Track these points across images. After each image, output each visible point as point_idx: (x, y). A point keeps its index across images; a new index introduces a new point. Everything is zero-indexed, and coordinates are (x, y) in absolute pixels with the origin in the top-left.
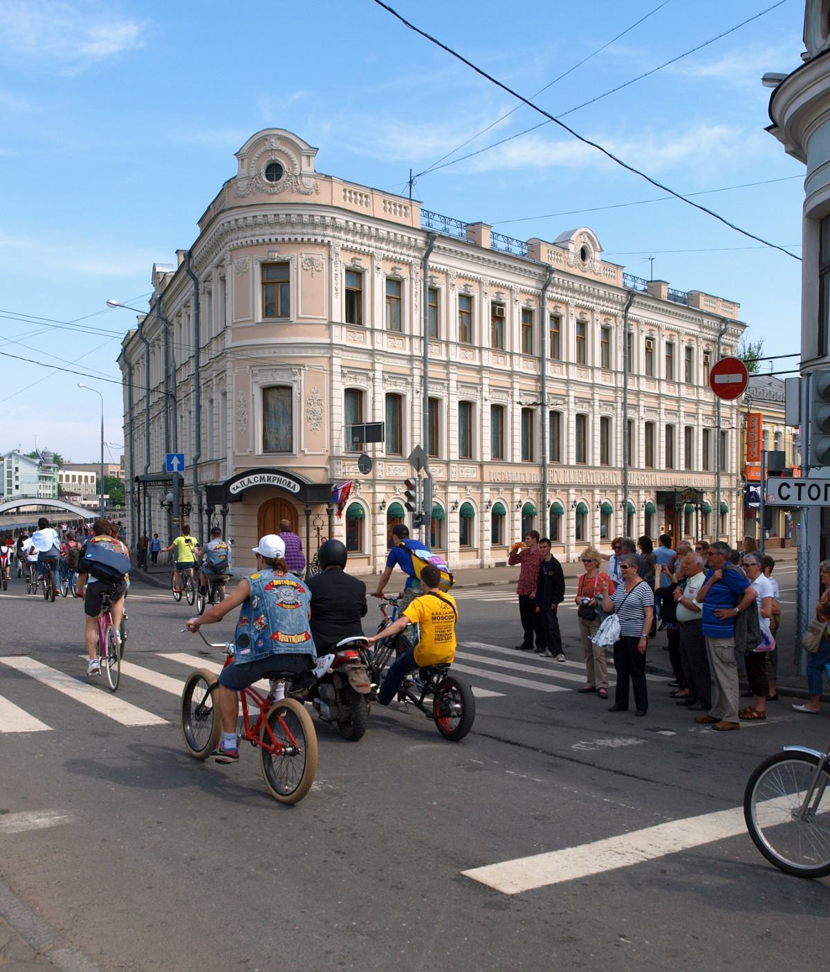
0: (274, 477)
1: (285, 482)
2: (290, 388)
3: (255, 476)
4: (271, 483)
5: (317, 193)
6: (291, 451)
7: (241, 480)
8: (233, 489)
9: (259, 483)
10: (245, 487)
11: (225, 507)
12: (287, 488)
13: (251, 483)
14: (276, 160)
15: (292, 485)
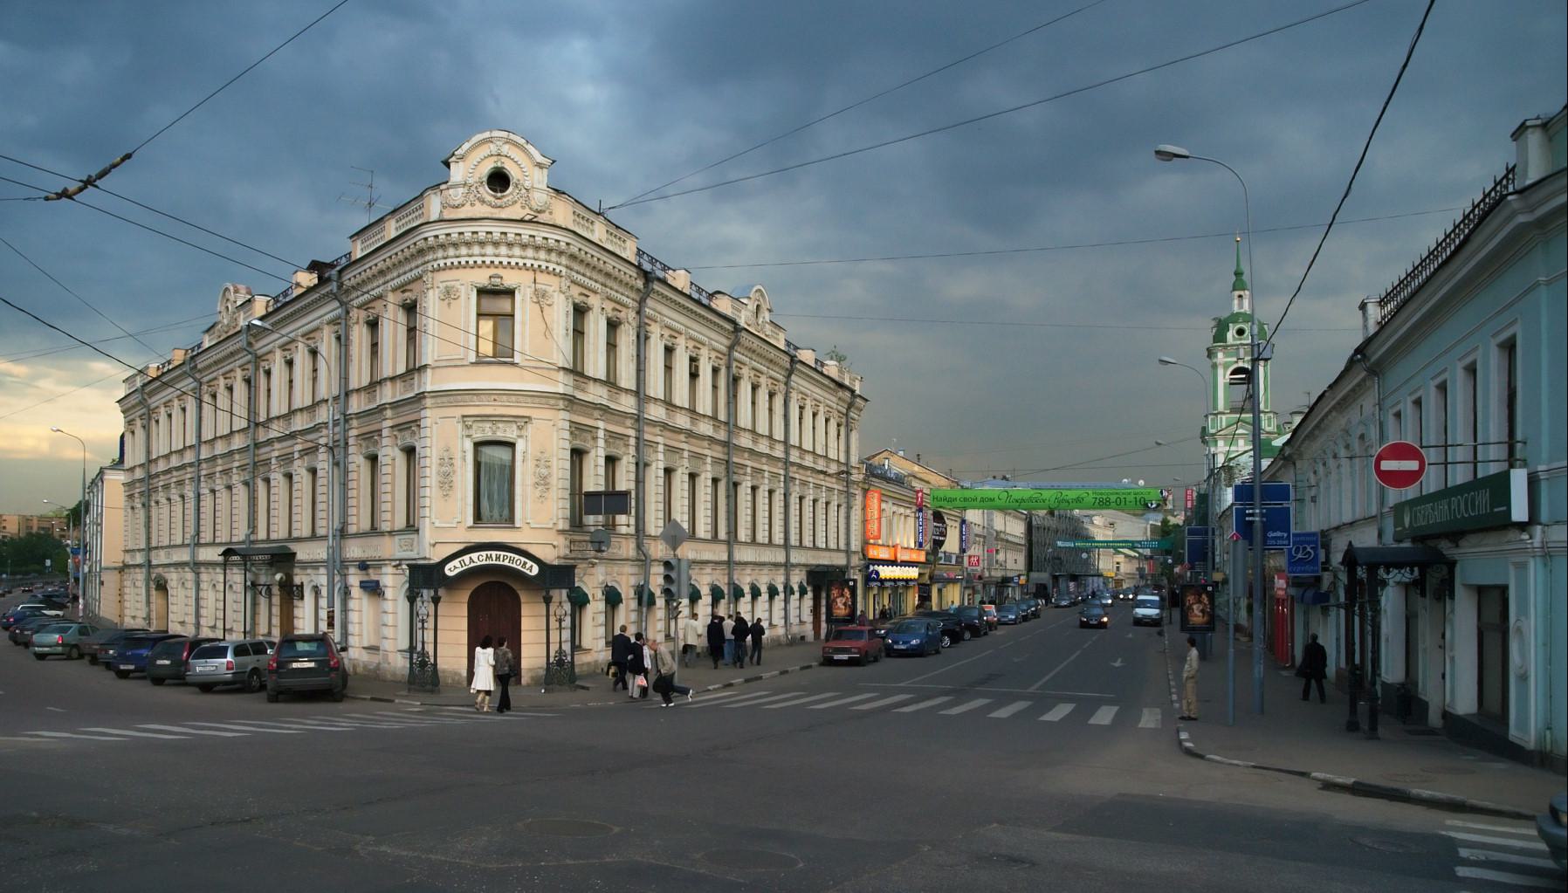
0: (504, 556)
1: (519, 562)
2: (512, 445)
3: (479, 553)
4: (501, 563)
5: (551, 213)
7: (460, 559)
8: (450, 569)
9: (484, 563)
10: (465, 568)
11: (436, 592)
12: (522, 569)
15: (527, 566)
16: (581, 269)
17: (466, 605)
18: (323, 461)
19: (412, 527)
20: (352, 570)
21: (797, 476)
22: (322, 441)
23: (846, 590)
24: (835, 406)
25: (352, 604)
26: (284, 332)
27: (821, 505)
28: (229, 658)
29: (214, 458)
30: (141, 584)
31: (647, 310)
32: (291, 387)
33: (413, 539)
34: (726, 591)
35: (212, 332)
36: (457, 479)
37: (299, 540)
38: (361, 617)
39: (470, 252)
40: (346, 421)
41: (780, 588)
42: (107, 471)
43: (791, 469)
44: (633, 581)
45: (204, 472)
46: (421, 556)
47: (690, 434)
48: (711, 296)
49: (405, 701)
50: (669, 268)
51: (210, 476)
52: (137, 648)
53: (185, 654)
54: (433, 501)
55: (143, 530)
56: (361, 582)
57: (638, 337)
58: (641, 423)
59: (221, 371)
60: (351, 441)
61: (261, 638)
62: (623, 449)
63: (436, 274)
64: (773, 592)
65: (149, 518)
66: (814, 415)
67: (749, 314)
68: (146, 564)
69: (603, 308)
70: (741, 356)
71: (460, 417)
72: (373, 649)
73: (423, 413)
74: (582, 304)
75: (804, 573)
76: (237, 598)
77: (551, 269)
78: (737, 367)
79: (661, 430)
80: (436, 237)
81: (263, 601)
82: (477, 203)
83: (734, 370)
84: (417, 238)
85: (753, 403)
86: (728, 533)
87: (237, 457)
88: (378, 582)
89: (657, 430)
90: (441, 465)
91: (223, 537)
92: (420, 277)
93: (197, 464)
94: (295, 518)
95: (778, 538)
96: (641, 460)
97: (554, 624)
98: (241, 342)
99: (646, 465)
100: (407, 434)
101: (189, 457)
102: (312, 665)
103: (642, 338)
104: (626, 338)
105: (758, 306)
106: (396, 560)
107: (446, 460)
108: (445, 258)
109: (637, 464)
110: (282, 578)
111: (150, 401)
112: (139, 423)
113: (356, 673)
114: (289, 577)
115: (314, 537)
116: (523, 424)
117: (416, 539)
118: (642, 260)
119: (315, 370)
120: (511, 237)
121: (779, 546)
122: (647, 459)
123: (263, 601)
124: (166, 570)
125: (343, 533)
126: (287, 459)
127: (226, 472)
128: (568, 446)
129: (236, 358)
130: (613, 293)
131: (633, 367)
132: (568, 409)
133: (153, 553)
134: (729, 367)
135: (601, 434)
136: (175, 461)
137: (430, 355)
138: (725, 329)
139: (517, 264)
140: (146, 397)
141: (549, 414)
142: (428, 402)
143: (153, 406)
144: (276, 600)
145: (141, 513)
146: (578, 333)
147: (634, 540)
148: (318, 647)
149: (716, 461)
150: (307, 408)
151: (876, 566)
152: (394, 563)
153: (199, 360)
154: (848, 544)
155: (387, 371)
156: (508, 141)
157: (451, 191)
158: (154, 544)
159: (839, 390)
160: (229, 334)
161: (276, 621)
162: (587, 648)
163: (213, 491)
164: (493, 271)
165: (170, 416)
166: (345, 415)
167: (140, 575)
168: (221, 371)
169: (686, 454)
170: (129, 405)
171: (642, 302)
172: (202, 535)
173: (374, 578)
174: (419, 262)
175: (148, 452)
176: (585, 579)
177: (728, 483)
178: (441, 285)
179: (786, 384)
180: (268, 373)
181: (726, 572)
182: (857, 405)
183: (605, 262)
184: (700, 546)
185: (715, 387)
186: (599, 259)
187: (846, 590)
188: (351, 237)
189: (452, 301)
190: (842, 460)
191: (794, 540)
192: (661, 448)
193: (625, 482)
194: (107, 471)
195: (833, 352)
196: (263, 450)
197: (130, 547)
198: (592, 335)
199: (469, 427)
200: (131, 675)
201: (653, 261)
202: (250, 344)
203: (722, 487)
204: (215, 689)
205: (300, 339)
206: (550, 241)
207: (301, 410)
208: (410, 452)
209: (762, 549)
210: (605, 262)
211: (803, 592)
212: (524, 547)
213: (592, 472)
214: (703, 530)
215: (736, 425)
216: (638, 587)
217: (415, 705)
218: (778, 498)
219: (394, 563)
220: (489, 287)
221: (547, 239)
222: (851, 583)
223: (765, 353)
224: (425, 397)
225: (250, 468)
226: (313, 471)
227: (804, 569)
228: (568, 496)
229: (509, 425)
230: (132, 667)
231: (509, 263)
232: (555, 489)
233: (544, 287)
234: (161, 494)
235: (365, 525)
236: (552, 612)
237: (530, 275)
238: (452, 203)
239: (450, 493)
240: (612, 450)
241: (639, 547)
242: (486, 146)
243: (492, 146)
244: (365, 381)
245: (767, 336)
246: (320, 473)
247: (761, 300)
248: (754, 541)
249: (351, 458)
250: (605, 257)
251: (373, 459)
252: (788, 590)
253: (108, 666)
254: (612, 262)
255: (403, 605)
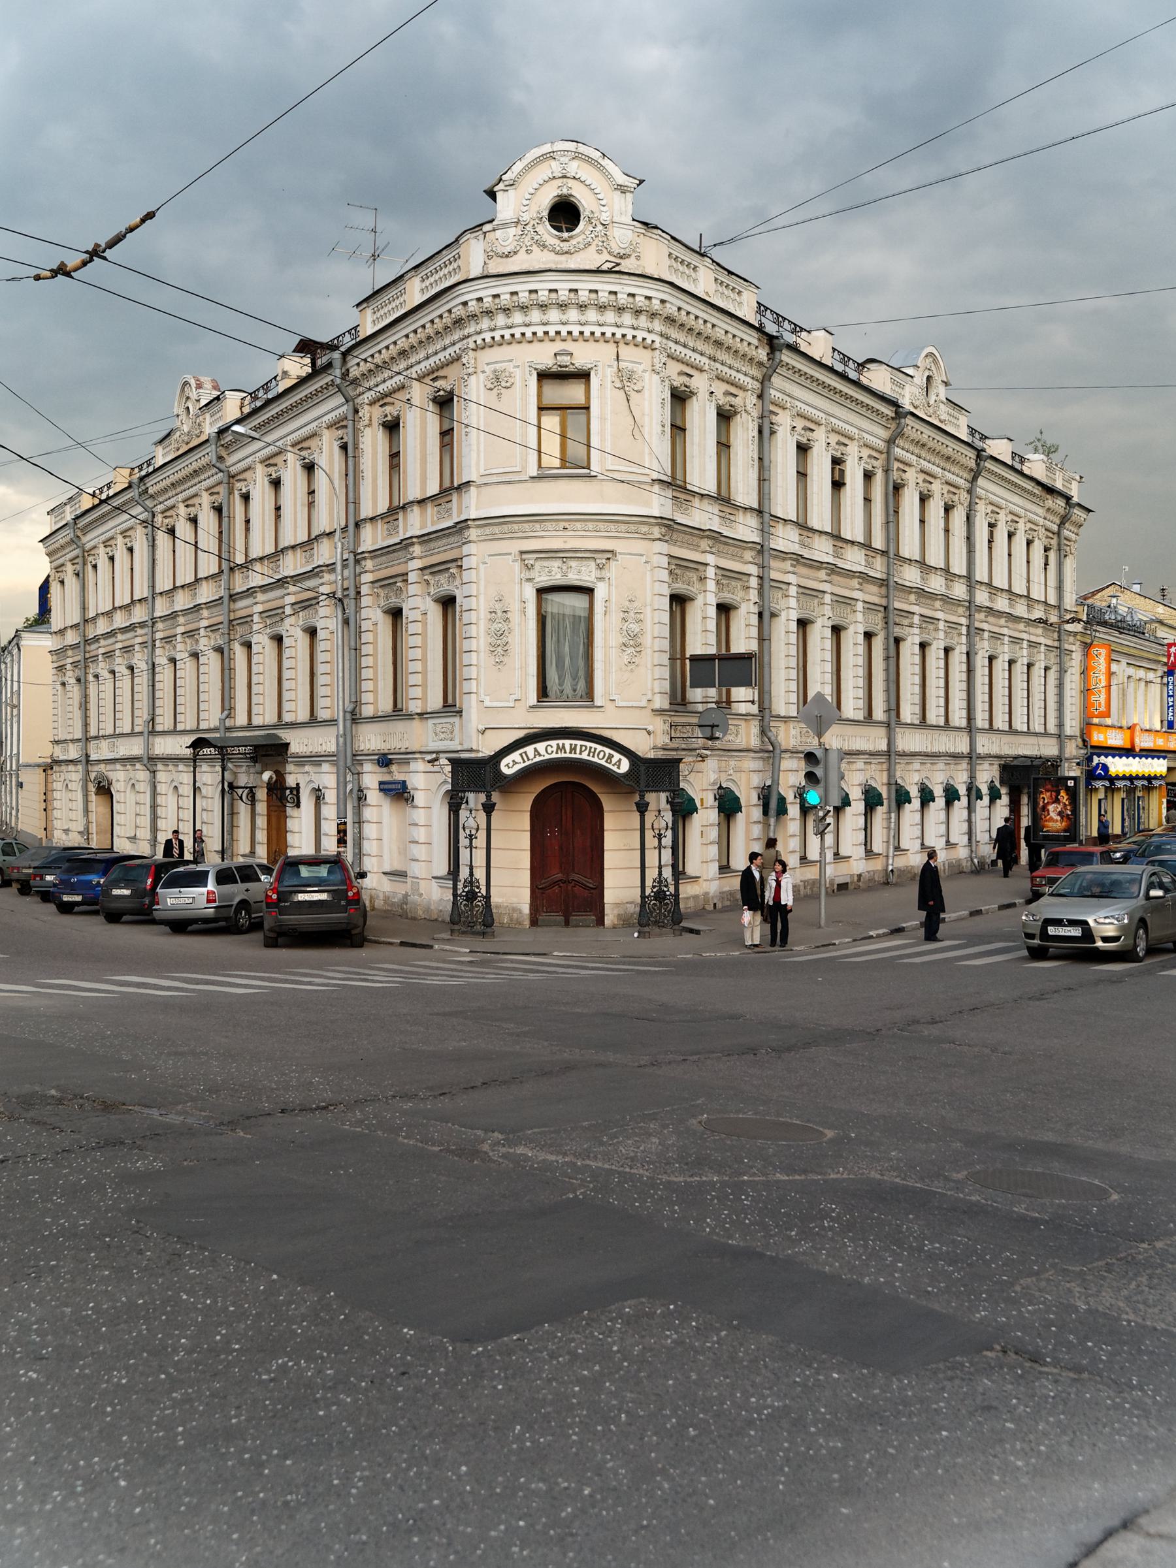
0: (581, 746)
1: (601, 755)
2: (589, 591)
4: (578, 756)
5: (638, 258)
6: (589, 695)
8: (507, 765)
9: (554, 756)
10: (530, 762)
11: (489, 797)
13: (540, 755)
14: (571, 195)
15: (614, 760)
16: (681, 336)
17: (528, 814)
18: (327, 619)
19: (451, 707)
20: (368, 767)
21: (985, 626)
22: (325, 589)
23: (1063, 793)
24: (1041, 521)
25: (368, 813)
26: (269, 438)
27: (1020, 668)
28: (211, 885)
29: (173, 615)
30: (77, 787)
31: (773, 392)
32: (278, 517)
33: (453, 724)
34: (885, 795)
35: (166, 442)
36: (514, 640)
37: (292, 725)
38: (380, 831)
39: (527, 320)
40: (357, 562)
41: (962, 790)
42: (23, 635)
43: (977, 616)
44: (756, 780)
45: (159, 635)
46: (465, 747)
47: (833, 570)
48: (861, 366)
49: (448, 947)
50: (802, 329)
51: (169, 640)
52: (83, 873)
53: (149, 881)
54: (482, 671)
55: (77, 714)
56: (381, 783)
57: (760, 432)
58: (766, 554)
59: (181, 497)
60: (365, 590)
61: (241, 860)
62: (741, 594)
63: (480, 353)
64: (951, 795)
65: (86, 697)
66: (1011, 535)
67: (916, 391)
68: (83, 759)
69: (712, 393)
70: (904, 453)
71: (517, 553)
72: (398, 875)
73: (466, 549)
74: (683, 388)
75: (996, 767)
76: (211, 801)
77: (639, 339)
78: (899, 469)
79: (792, 565)
80: (480, 300)
81: (243, 809)
82: (535, 248)
83: (895, 475)
84: (452, 302)
85: (922, 521)
86: (888, 711)
87: (205, 613)
88: (404, 782)
89: (787, 565)
90: (492, 621)
91: (187, 721)
92: (459, 358)
93: (150, 623)
94: (286, 696)
95: (959, 718)
96: (766, 607)
97: (651, 842)
98: (209, 454)
99: (773, 615)
100: (443, 578)
101: (139, 614)
102: (324, 896)
103: (765, 432)
104: (744, 433)
105: (929, 378)
106: (434, 752)
107: (499, 614)
108: (493, 330)
109: (760, 615)
110: (271, 778)
111: (84, 539)
112: (69, 568)
113: (373, 909)
114: (280, 776)
115: (313, 721)
116: (604, 561)
117: (457, 724)
118: (763, 320)
119: (311, 493)
120: (584, 296)
121: (959, 729)
122: (774, 607)
123: (243, 809)
124: (109, 767)
125: (355, 717)
126: (274, 614)
127: (191, 634)
128: (667, 592)
129: (202, 477)
130: (726, 369)
131: (753, 475)
132: (667, 538)
133: (93, 744)
134: (887, 471)
135: (711, 572)
136: (120, 620)
137: (474, 469)
138: (882, 415)
139: (592, 333)
140: (79, 534)
141: (639, 546)
142: (473, 533)
143: (88, 546)
144: (261, 808)
145: (75, 691)
146: (678, 429)
147: (757, 723)
148: (329, 872)
149: (870, 607)
150: (301, 545)
151: (1103, 757)
152: (429, 757)
153: (150, 482)
154: (1061, 725)
155: (413, 491)
156: (577, 156)
157: (498, 233)
158: (93, 732)
159: (1048, 496)
160: (191, 445)
161: (261, 836)
162: (694, 875)
163: (173, 661)
164: (558, 346)
165: (112, 559)
166: (356, 554)
167: (75, 775)
168: (181, 497)
169: (828, 598)
170: (57, 545)
171: (765, 381)
172: (158, 720)
173: (399, 777)
174: (457, 336)
175: (84, 608)
176: (691, 778)
177: (887, 638)
178: (487, 368)
179: (970, 491)
180: (246, 498)
181: (885, 766)
182: (1073, 518)
183: (713, 326)
184: (849, 730)
185: (867, 500)
186: (705, 322)
187: (1063, 793)
188: (358, 305)
189: (503, 390)
190: (1052, 600)
191: (981, 721)
192: (793, 590)
193: (743, 641)
194: (23, 635)
195: (1039, 440)
196: (241, 604)
197: (61, 737)
198: (696, 432)
199: (529, 568)
200: (77, 909)
201: (779, 319)
202: (220, 458)
203: (878, 643)
204: (190, 928)
205: (289, 448)
206: (637, 298)
207: (293, 547)
208: (448, 603)
209: (936, 734)
210: (713, 326)
211: (994, 796)
212: (606, 734)
213: (699, 628)
214: (852, 707)
215: (897, 555)
216: (763, 788)
217: (462, 950)
218: (958, 659)
219: (429, 757)
220: (555, 369)
221: (633, 295)
222: (1071, 783)
223: (939, 448)
224: (468, 527)
225: (224, 628)
226: (312, 632)
227: (997, 762)
228: (667, 662)
229: (585, 563)
230: (78, 898)
231: (581, 333)
232: (649, 651)
233: (630, 366)
234: (102, 665)
235: (386, 705)
236: (648, 825)
237: (611, 347)
238: (500, 250)
239: (505, 659)
240: (725, 594)
241: (763, 732)
242: (546, 164)
243: (553, 163)
244: (383, 507)
245: (941, 421)
246: (321, 634)
247: (933, 368)
248: (923, 722)
249: (364, 613)
250: (714, 317)
251: (396, 614)
252: (973, 792)
253: (46, 896)
254: (723, 323)
255: (440, 815)
